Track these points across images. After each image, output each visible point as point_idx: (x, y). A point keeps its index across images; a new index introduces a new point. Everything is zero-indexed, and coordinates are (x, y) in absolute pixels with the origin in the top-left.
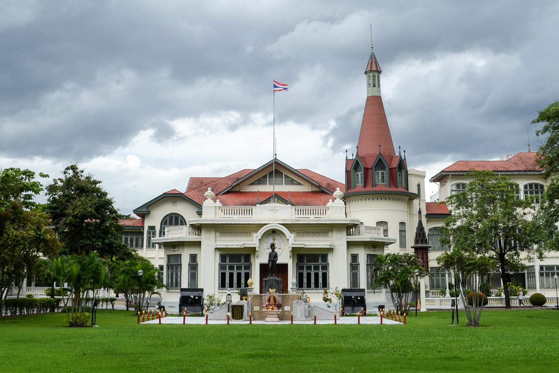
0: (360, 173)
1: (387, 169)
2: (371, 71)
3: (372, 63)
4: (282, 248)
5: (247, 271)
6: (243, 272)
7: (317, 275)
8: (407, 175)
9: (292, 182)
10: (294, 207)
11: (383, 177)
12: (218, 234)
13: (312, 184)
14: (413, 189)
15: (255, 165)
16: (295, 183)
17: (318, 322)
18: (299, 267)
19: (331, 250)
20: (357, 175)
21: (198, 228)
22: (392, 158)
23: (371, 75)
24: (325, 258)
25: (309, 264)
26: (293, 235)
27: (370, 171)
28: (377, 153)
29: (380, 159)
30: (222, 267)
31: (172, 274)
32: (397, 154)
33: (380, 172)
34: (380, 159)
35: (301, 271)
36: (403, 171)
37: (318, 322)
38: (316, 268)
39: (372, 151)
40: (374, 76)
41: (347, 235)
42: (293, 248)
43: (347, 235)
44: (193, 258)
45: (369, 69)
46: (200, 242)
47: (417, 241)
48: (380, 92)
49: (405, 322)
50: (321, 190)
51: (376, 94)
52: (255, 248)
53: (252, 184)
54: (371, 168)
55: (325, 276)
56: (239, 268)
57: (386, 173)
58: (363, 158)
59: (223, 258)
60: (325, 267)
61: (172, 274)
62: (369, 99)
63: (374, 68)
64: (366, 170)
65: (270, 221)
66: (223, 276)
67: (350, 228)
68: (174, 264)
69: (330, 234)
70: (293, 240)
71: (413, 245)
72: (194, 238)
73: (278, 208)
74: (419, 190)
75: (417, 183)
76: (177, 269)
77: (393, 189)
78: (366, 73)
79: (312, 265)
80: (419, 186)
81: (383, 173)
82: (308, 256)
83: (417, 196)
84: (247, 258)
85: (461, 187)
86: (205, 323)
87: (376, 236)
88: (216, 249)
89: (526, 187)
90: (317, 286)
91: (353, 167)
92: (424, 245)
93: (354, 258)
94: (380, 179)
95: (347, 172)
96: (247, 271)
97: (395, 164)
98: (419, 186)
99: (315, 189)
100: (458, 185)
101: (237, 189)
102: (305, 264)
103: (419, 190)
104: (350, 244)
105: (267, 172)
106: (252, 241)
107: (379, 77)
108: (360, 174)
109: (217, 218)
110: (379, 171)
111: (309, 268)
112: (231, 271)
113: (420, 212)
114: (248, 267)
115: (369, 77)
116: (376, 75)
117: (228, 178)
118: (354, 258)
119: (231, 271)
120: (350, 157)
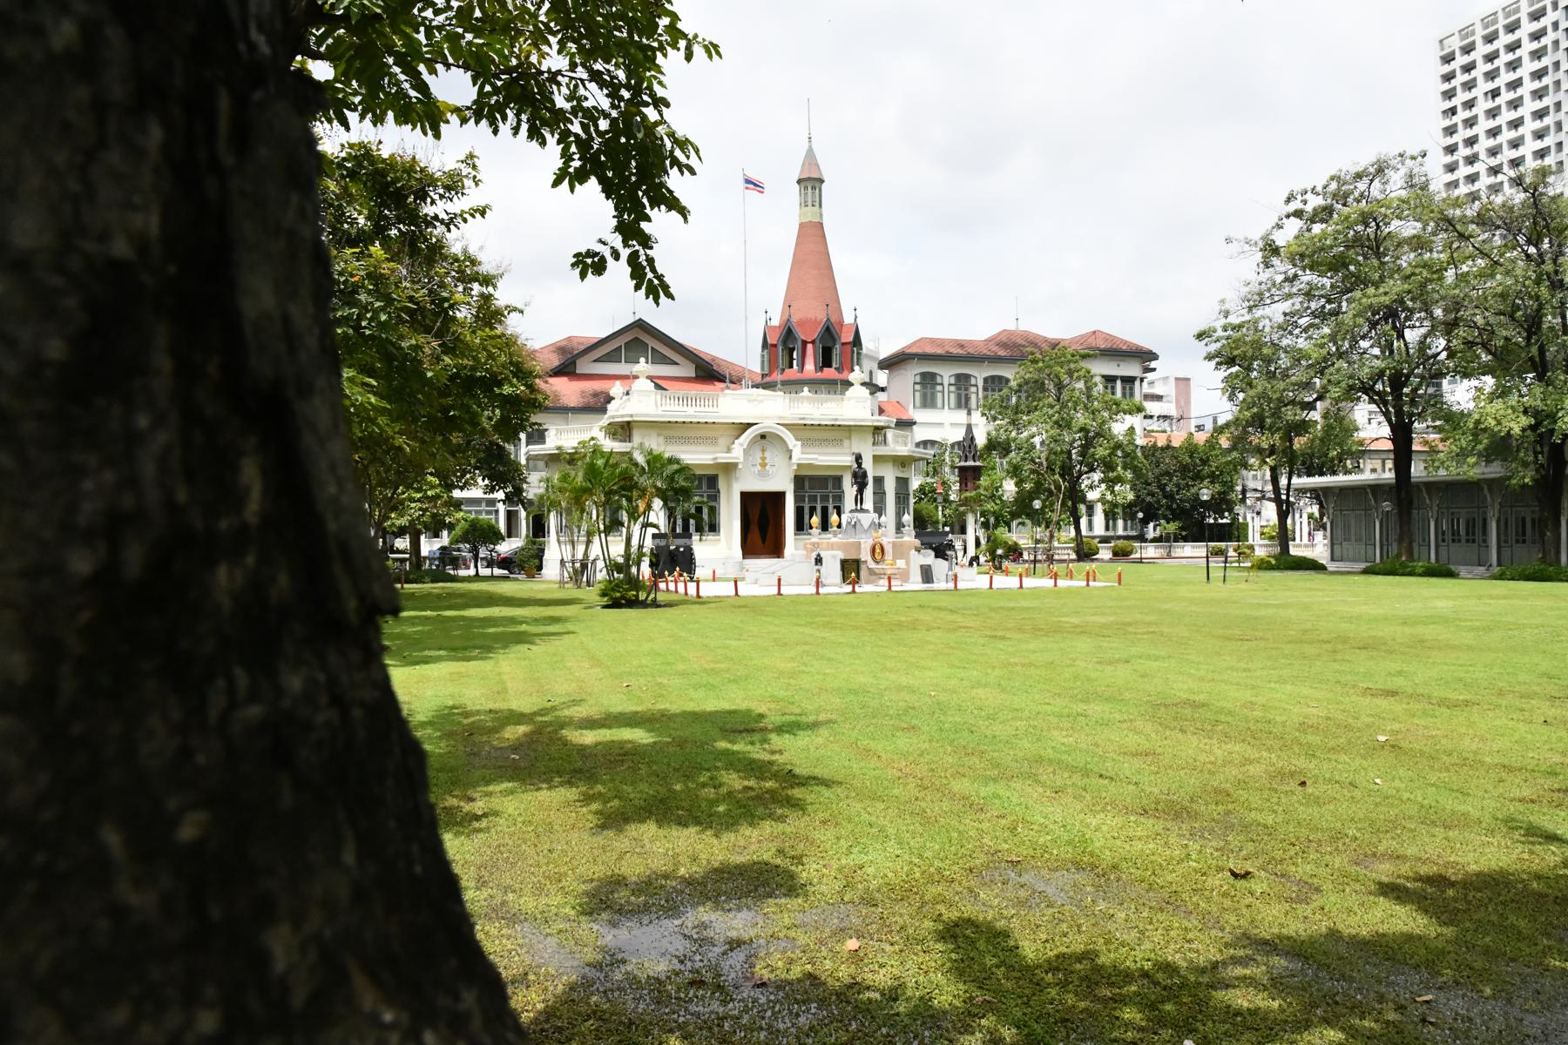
21: (623, 430)
22: (841, 324)
27: (810, 346)
32: (848, 319)
38: (825, 498)
39: (811, 313)
52: (736, 465)
54: (813, 342)
62: (802, 225)
69: (846, 442)
78: (799, 182)
82: (812, 479)
84: (712, 481)
100: (923, 375)
105: (620, 342)
106: (737, 453)
110: (814, 347)
111: (813, 499)
114: (715, 497)
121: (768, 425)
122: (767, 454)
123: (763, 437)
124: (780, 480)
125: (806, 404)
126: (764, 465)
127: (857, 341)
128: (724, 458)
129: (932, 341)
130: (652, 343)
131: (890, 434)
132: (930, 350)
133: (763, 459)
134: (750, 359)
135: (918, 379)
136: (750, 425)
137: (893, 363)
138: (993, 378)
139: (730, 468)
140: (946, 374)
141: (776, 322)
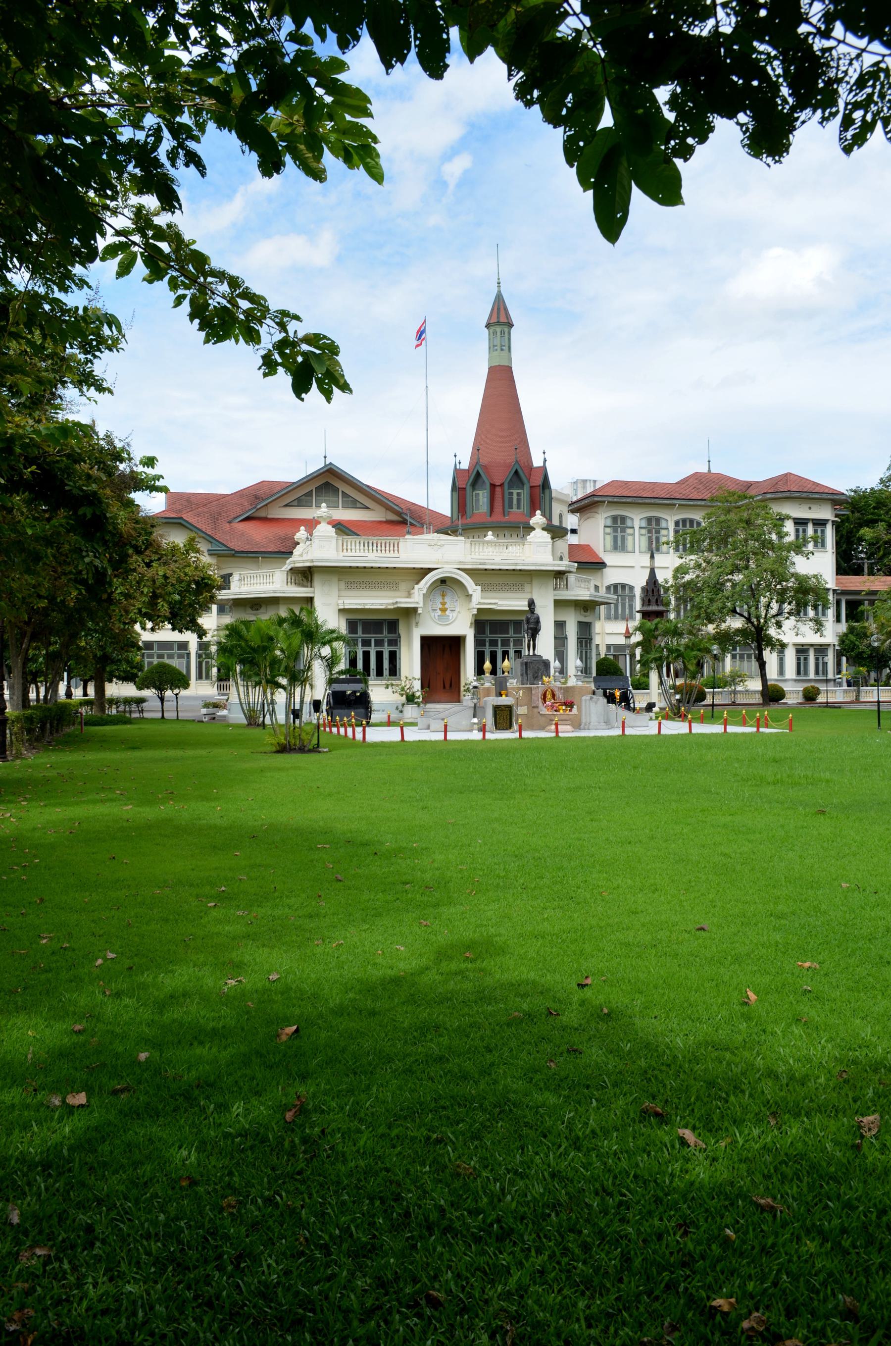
0: (481, 493)
1: (526, 488)
2: (499, 323)
3: (499, 309)
4: (457, 609)
5: (392, 648)
6: (386, 650)
8: (551, 498)
9: (353, 504)
11: (519, 500)
13: (388, 508)
15: (294, 472)
16: (359, 505)
17: (628, 732)
20: (477, 495)
21: (305, 575)
23: (498, 329)
25: (494, 636)
26: (479, 588)
27: (498, 490)
29: (516, 472)
32: (537, 462)
33: (515, 492)
34: (516, 472)
35: (481, 649)
36: (547, 491)
37: (628, 732)
38: (505, 643)
39: (500, 457)
40: (502, 332)
41: (555, 589)
42: (479, 610)
43: (555, 589)
45: (494, 320)
46: (310, 600)
48: (510, 359)
49: (791, 729)
50: (403, 518)
51: (505, 363)
52: (415, 610)
53: (286, 505)
54: (502, 485)
56: (379, 643)
57: (525, 493)
58: (485, 467)
62: (492, 370)
63: (503, 319)
64: (493, 486)
65: (438, 563)
69: (527, 587)
70: (480, 598)
72: (301, 592)
73: (442, 543)
74: (561, 522)
75: (558, 512)
79: (499, 637)
80: (561, 516)
81: (518, 494)
84: (393, 626)
85: (654, 523)
86: (399, 738)
88: (340, 610)
89: (677, 523)
92: (661, 608)
96: (392, 648)
98: (561, 516)
99: (394, 517)
100: (614, 519)
101: (262, 514)
102: (488, 636)
103: (561, 522)
106: (416, 597)
107: (509, 334)
108: (483, 496)
111: (494, 643)
112: (366, 649)
114: (395, 642)
115: (495, 333)
116: (506, 330)
117: (240, 494)
119: (366, 649)
121: (447, 570)
122: (447, 599)
123: (443, 581)
124: (459, 623)
125: (491, 549)
126: (444, 610)
127: (546, 484)
128: (405, 602)
129: (625, 484)
130: (342, 487)
131: (572, 578)
133: (443, 604)
134: (442, 503)
135: (609, 522)
136: (430, 570)
137: (585, 506)
138: (684, 521)
139: (410, 613)
140: (637, 518)
141: (465, 465)
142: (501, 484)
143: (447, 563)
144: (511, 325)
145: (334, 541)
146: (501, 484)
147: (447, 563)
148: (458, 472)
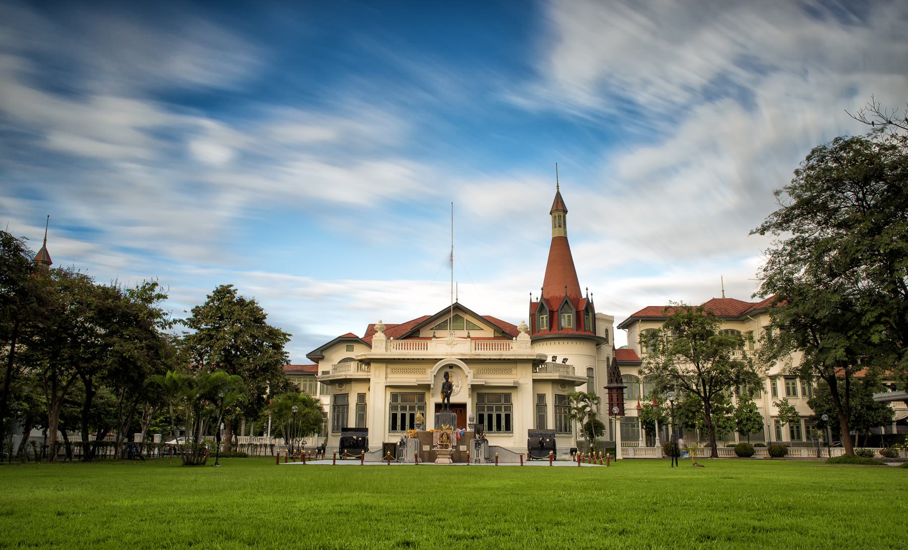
1: (574, 311)
7: (499, 416)
10: (473, 342)
11: (569, 320)
12: (389, 371)
14: (601, 333)
18: (479, 408)
19: (514, 388)
23: (556, 214)
24: (508, 397)
28: (563, 295)
30: (393, 407)
31: (338, 416)
32: (584, 296)
36: (590, 314)
38: (499, 409)
39: (558, 292)
42: (472, 385)
44: (362, 397)
46: (369, 380)
47: (610, 381)
48: (565, 232)
52: (429, 385)
55: (508, 417)
57: (572, 316)
58: (547, 301)
59: (394, 397)
60: (509, 408)
61: (338, 416)
62: (553, 239)
64: (552, 313)
66: (394, 417)
67: (537, 363)
68: (340, 405)
69: (514, 371)
71: (606, 385)
72: (361, 375)
74: (607, 335)
75: (604, 328)
76: (343, 410)
77: (581, 333)
80: (607, 331)
81: (569, 317)
83: (606, 340)
84: (422, 398)
87: (565, 374)
90: (499, 428)
91: (536, 309)
92: (619, 385)
93: (541, 398)
94: (567, 321)
95: (532, 316)
97: (582, 307)
98: (607, 331)
104: (535, 381)
107: (564, 217)
108: (545, 317)
109: (389, 352)
113: (608, 359)
114: (422, 408)
115: (555, 217)
118: (541, 398)
120: (534, 300)
121: (453, 360)
130: (467, 317)
132: (650, 314)
136: (437, 360)
137: (627, 325)
142: (564, 310)
143: (453, 355)
144: (565, 212)
145: (384, 343)
146: (564, 310)
147: (453, 355)
148: (532, 305)
